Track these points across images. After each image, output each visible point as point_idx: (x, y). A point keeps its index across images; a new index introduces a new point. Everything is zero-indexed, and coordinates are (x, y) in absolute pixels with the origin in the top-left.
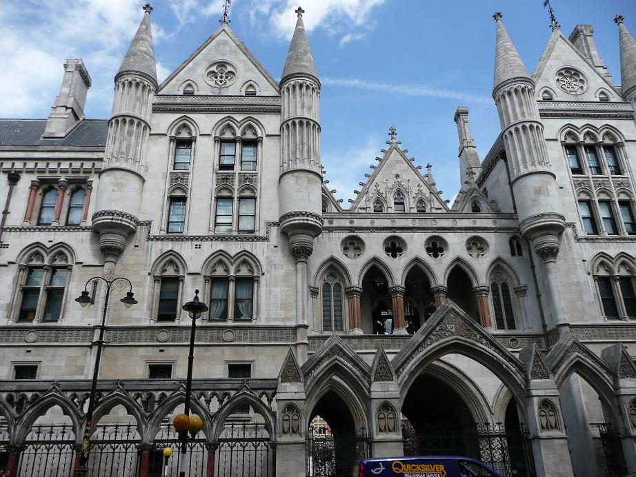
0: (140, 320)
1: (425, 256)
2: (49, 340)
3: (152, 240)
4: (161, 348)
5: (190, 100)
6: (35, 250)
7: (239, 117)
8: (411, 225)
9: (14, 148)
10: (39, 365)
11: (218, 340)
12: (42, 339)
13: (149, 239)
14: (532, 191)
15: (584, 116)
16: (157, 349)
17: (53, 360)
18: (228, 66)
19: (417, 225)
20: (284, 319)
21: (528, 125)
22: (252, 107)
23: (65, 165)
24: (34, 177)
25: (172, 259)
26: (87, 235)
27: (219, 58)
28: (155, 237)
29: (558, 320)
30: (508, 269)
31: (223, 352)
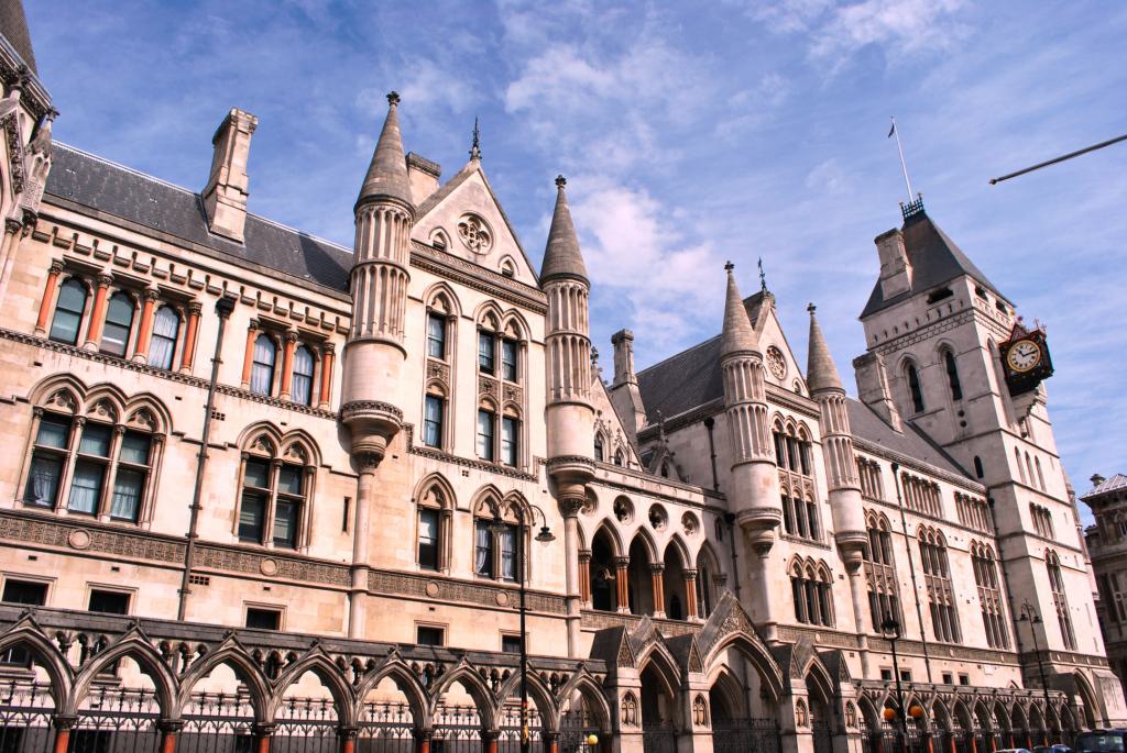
0: (406, 563)
1: (648, 525)
2: (293, 576)
3: (414, 452)
4: (432, 604)
5: (438, 256)
6: (267, 434)
7: (505, 306)
8: (639, 486)
9: (223, 257)
10: (51, 583)
11: (491, 602)
12: (284, 572)
13: (410, 449)
14: (761, 481)
15: (788, 406)
16: (427, 606)
17: (302, 603)
18: (482, 225)
19: (644, 488)
20: (555, 585)
21: (754, 406)
22: (518, 297)
23: (299, 308)
24: (255, 313)
25: (439, 486)
26: (332, 425)
27: (474, 209)
28: (418, 450)
29: (768, 618)
30: (711, 554)
31: (497, 619)
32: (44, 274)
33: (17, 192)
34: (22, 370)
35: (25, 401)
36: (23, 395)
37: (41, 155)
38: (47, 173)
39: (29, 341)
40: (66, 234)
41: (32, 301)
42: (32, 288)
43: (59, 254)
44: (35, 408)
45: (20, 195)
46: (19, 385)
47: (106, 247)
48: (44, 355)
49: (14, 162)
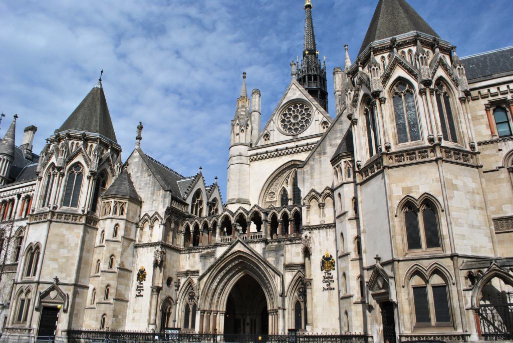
32: (484, 113)
33: (457, 86)
34: (494, 155)
35: (502, 167)
36: (501, 165)
37: (458, 67)
38: (464, 72)
39: (492, 142)
40: (484, 91)
41: (485, 126)
42: (482, 120)
43: (486, 101)
44: (508, 169)
45: (459, 86)
46: (497, 162)
47: (503, 88)
48: (501, 145)
49: (450, 76)
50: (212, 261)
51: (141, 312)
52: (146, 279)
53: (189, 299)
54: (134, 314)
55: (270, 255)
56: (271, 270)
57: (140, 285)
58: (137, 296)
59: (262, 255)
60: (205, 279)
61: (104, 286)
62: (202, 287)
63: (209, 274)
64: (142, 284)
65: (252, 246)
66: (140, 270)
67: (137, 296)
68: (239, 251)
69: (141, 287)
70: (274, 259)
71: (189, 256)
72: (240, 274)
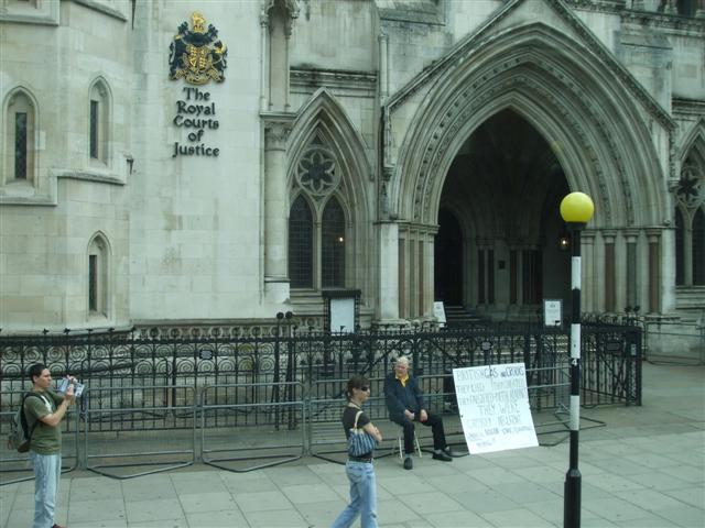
50: (430, 47)
51: (216, 228)
52: (227, 74)
53: (305, 178)
54: (173, 232)
55: (636, 59)
56: (639, 107)
57: (192, 102)
58: (179, 152)
59: (613, 52)
60: (411, 109)
61: (80, 84)
62: (399, 132)
63: (425, 90)
64: (206, 97)
65: (582, 16)
66: (183, 29)
67: (179, 152)
68: (540, 25)
69: (199, 109)
70: (648, 73)
71: (308, 8)
72: (493, 104)
